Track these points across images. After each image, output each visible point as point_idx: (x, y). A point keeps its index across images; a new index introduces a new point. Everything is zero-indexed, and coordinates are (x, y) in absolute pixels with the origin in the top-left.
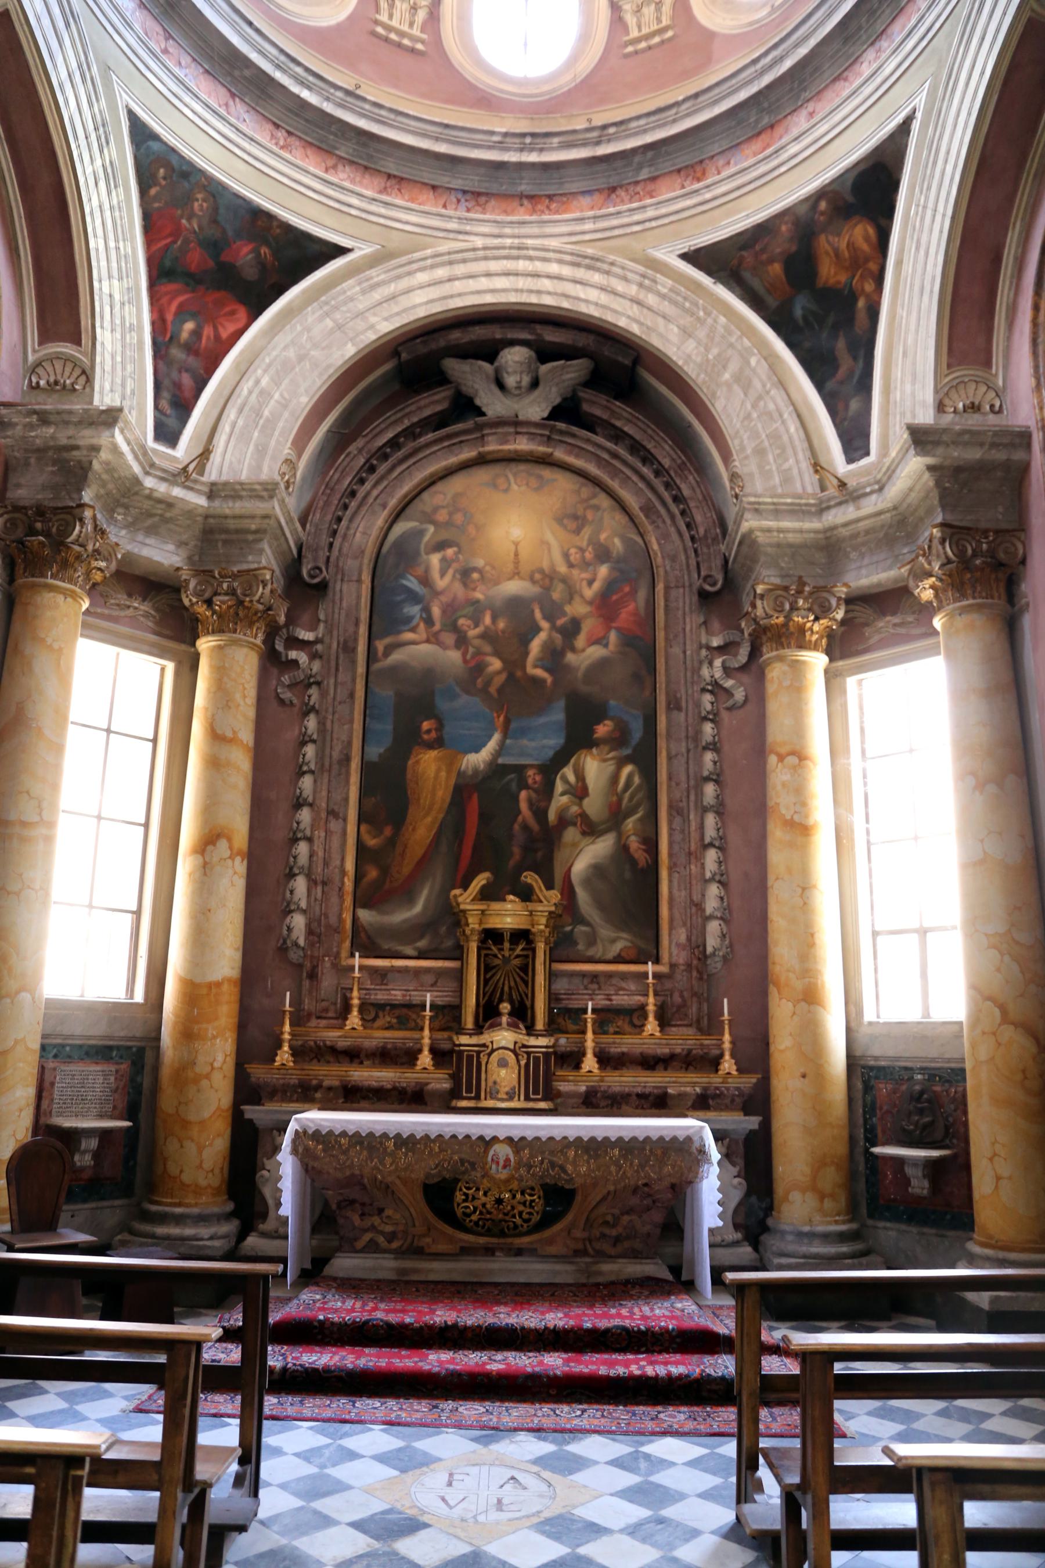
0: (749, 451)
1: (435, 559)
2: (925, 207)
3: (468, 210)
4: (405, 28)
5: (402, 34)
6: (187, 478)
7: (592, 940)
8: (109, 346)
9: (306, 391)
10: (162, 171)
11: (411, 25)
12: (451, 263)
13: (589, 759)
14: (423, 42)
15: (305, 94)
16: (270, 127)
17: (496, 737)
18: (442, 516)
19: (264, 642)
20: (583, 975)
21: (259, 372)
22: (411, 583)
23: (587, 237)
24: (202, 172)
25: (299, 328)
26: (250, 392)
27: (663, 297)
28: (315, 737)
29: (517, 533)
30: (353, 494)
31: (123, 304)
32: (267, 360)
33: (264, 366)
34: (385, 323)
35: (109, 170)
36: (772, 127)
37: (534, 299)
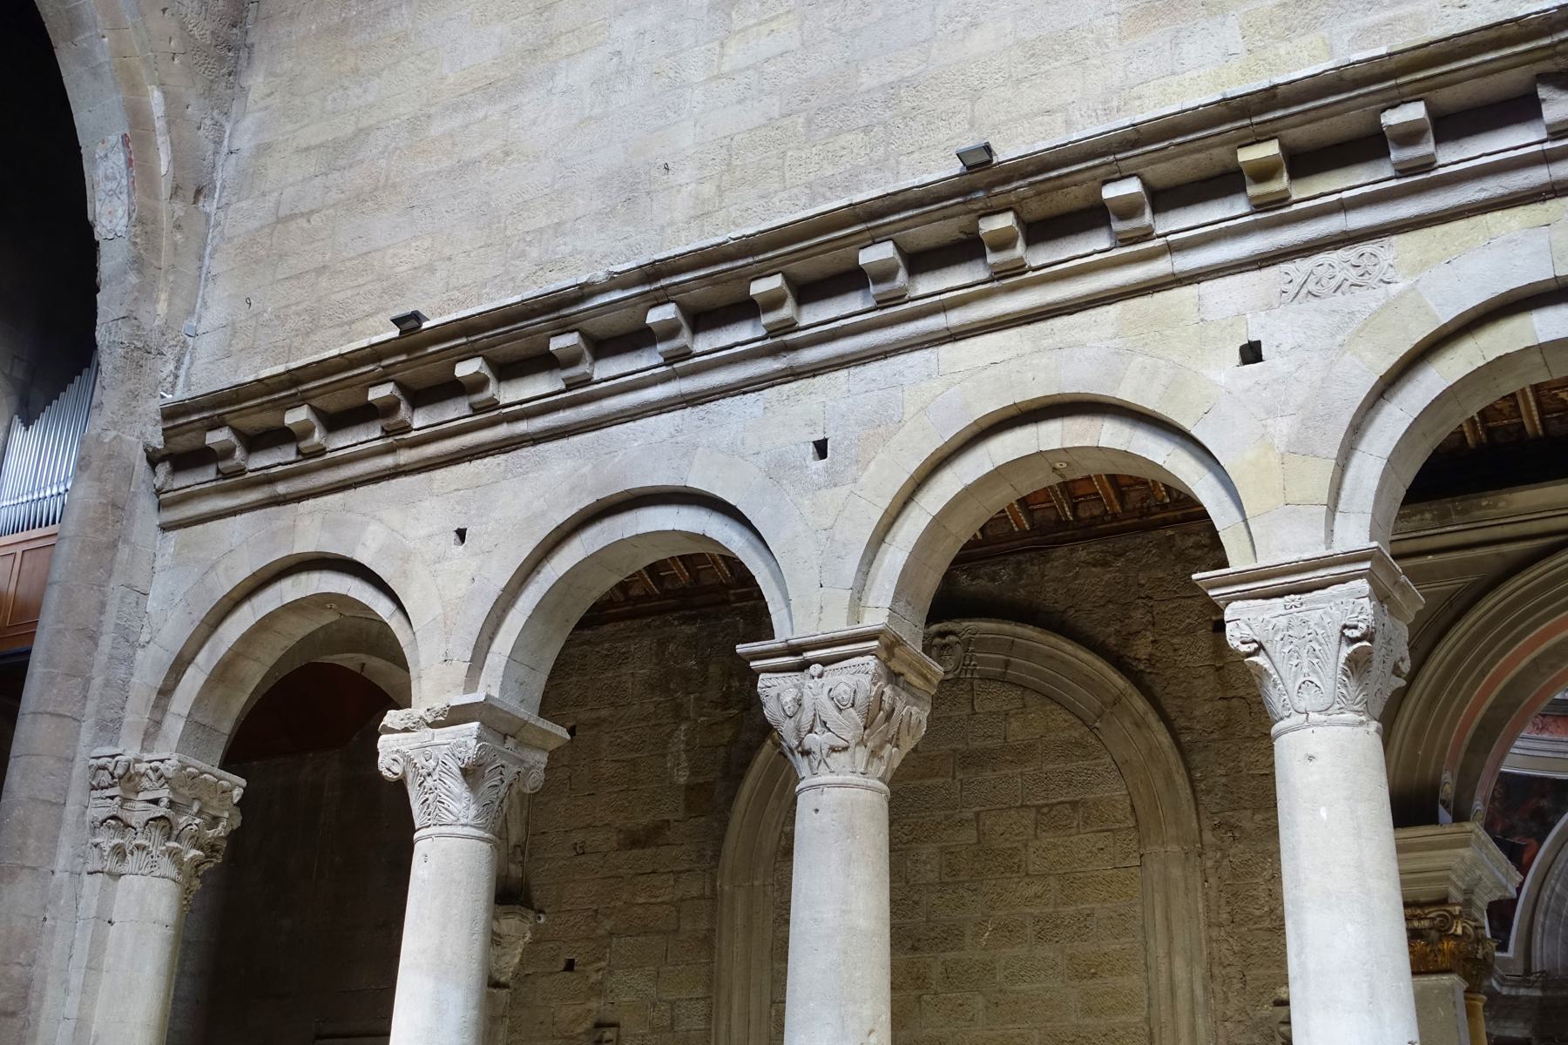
21: (1553, 882)
26: (1550, 898)
32: (1556, 872)
33: (1555, 877)
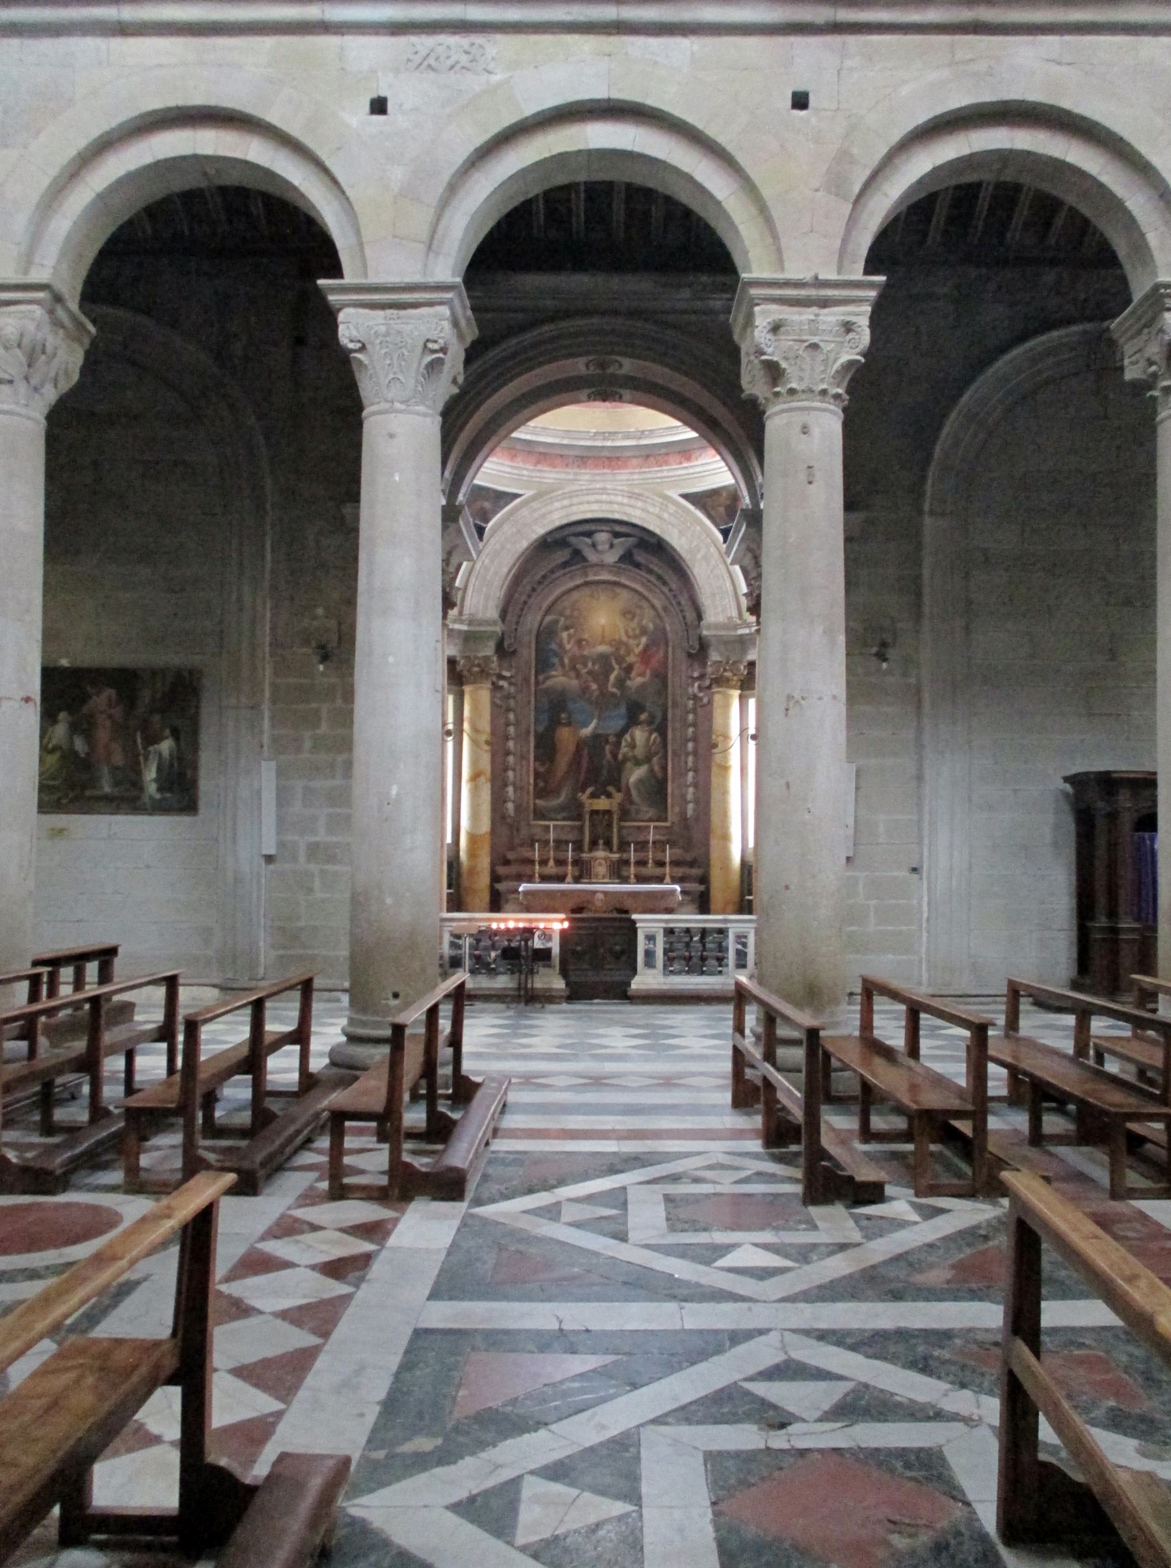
1: (565, 635)
7: (638, 812)
17: (595, 721)
18: (568, 612)
20: (634, 827)
22: (554, 646)
27: (671, 514)
29: (603, 621)
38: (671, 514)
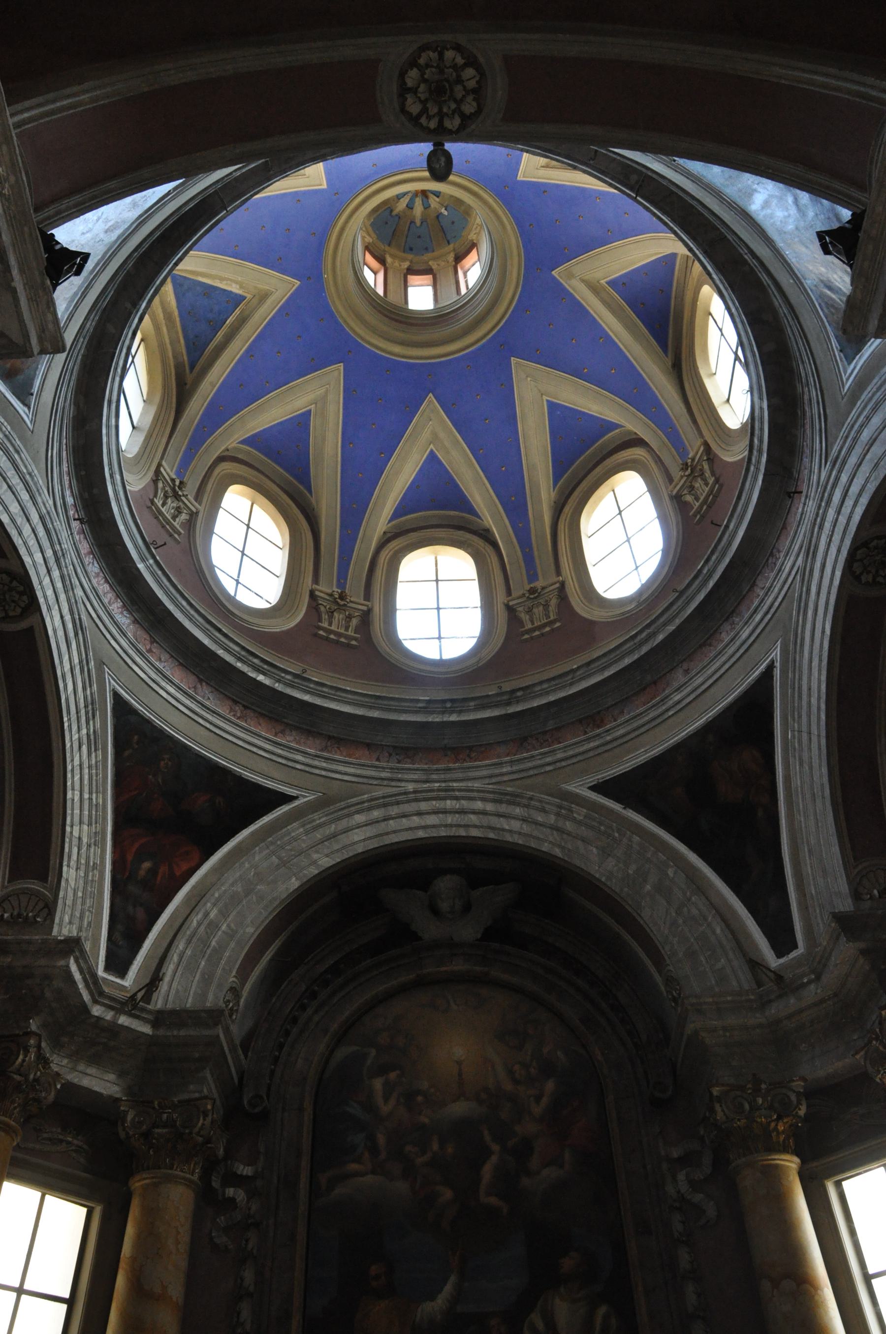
0: (681, 955)
1: (378, 1084)
2: (800, 731)
3: (399, 762)
4: (342, 631)
5: (340, 635)
6: (135, 1007)
8: (72, 883)
9: (252, 922)
10: (136, 737)
11: (347, 629)
12: (385, 805)
13: (557, 1301)
14: (356, 639)
15: (261, 678)
16: (229, 703)
17: (453, 1279)
19: (200, 1178)
21: (209, 905)
23: (506, 778)
24: (171, 738)
25: (247, 865)
26: (199, 924)
27: (579, 823)
28: (252, 1289)
29: (459, 1052)
30: (295, 1020)
31: (89, 846)
32: (217, 895)
33: (213, 901)
34: (327, 859)
35: (92, 737)
36: (655, 683)
37: (462, 832)
38: (579, 823)
